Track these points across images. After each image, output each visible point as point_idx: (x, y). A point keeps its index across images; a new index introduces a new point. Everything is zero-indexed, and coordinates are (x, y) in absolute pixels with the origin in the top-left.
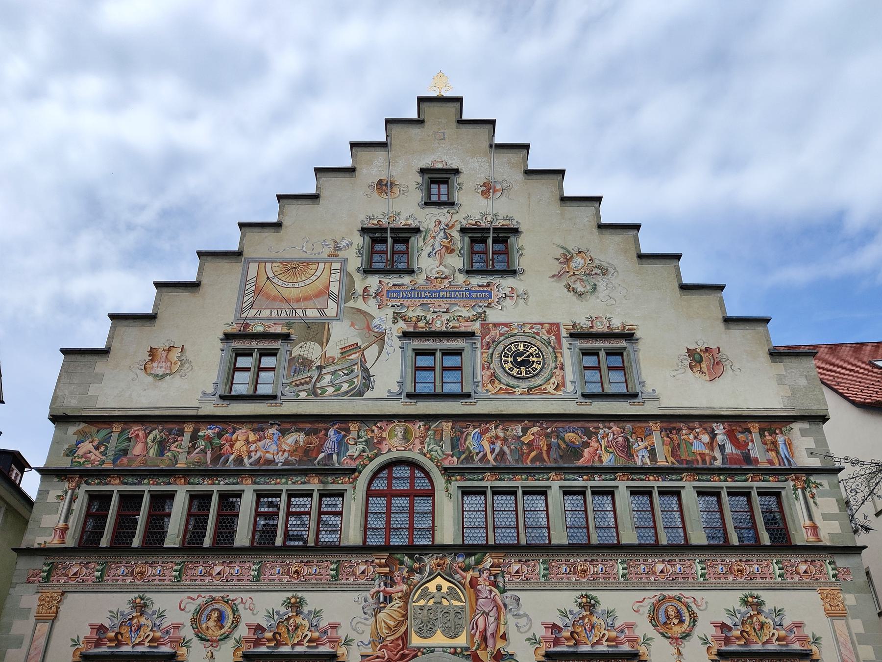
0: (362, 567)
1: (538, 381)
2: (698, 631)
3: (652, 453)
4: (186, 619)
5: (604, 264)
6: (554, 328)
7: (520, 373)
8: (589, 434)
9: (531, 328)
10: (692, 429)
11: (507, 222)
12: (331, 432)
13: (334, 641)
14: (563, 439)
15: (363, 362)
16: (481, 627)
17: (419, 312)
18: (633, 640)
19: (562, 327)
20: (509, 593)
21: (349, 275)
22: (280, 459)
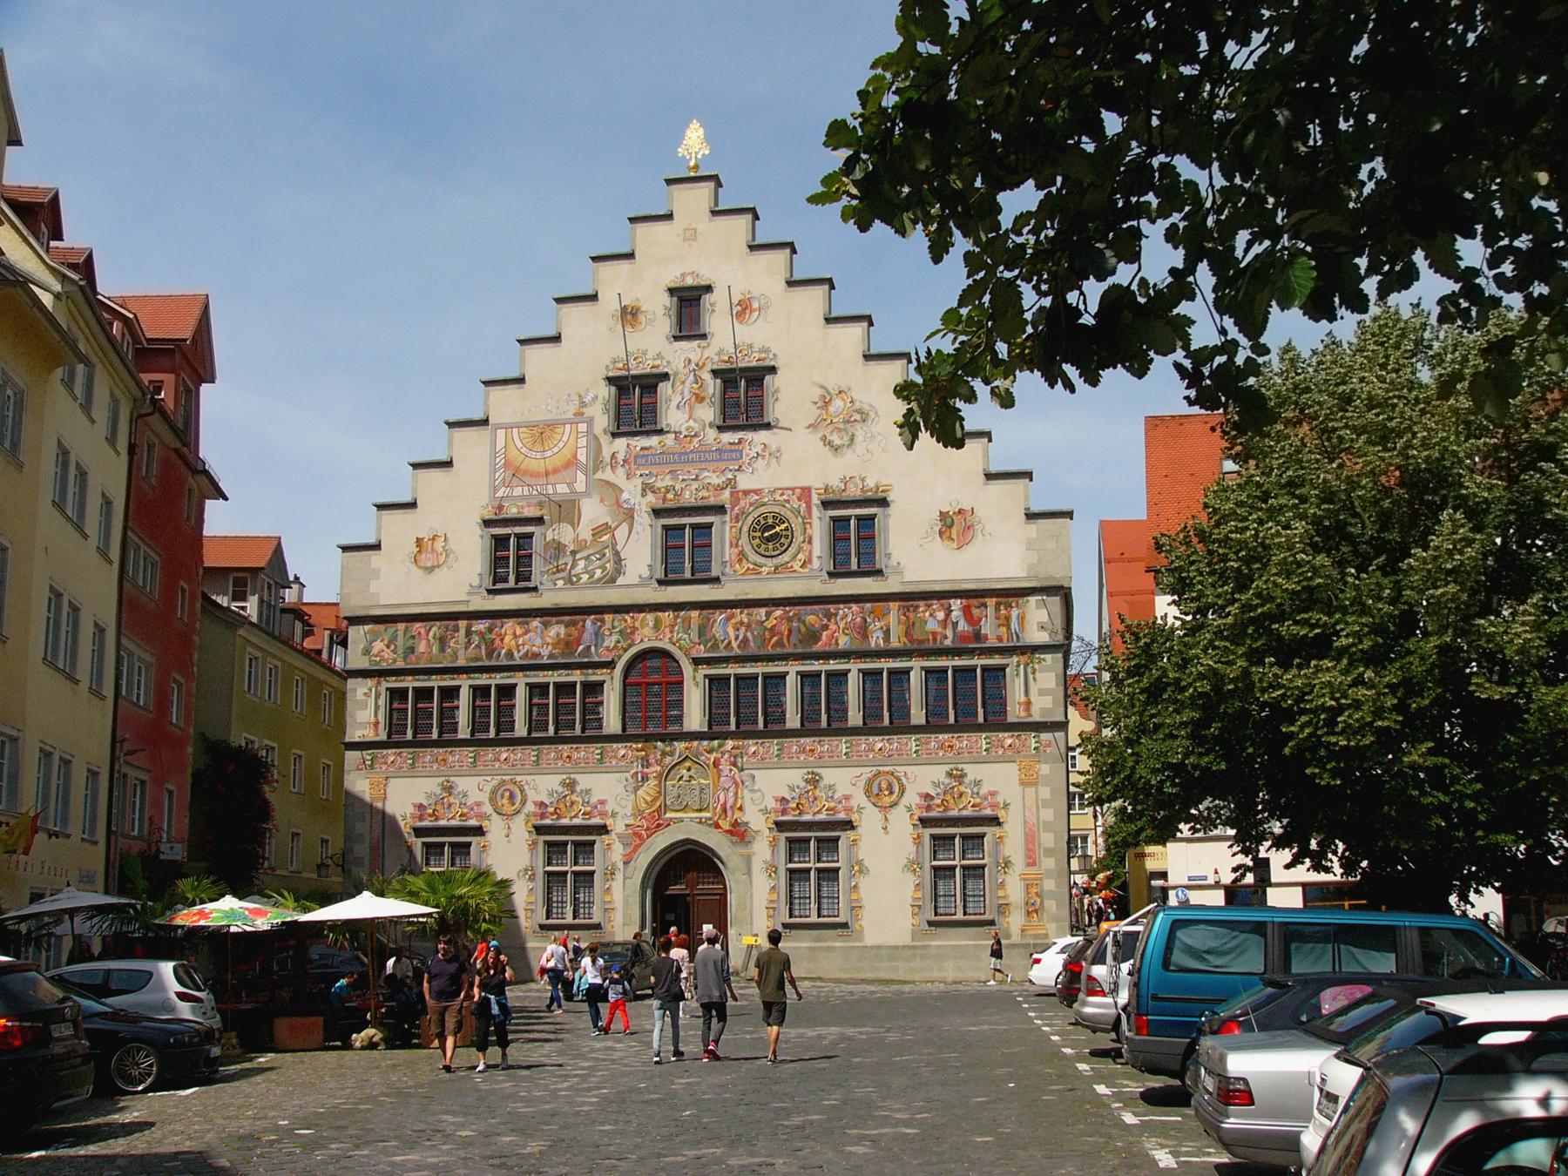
0: (622, 752)
1: (785, 557)
2: (905, 801)
3: (887, 633)
4: (484, 797)
5: (866, 407)
6: (806, 493)
7: (767, 550)
8: (829, 616)
9: (782, 495)
10: (929, 606)
11: (763, 355)
12: (588, 623)
13: (603, 814)
14: (804, 622)
15: (614, 544)
16: (722, 801)
17: (668, 482)
18: (848, 810)
19: (813, 492)
20: (746, 772)
21: (596, 437)
22: (545, 652)
